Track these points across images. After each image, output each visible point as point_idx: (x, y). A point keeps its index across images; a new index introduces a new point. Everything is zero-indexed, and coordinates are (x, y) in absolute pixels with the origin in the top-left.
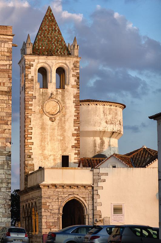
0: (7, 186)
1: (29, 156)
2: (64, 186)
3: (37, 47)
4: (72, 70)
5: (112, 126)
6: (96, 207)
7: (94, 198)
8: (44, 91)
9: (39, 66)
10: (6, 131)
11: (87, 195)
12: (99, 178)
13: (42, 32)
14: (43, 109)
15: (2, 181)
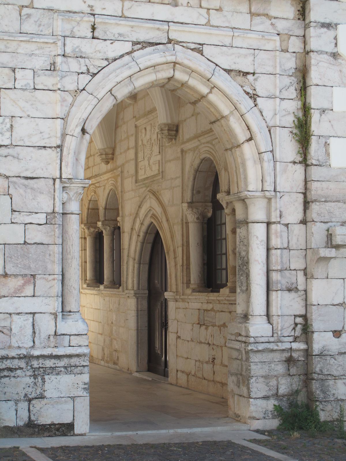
6: (327, 145)
7: (314, 76)
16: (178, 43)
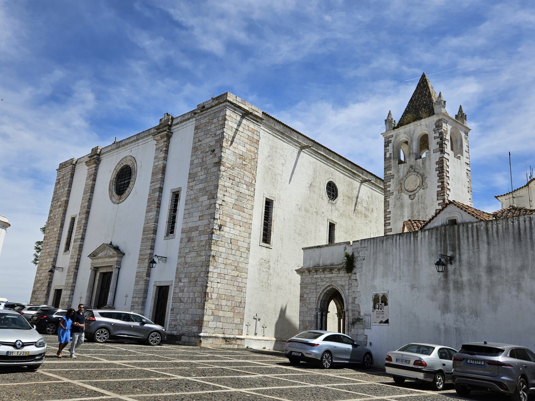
11: (346, 281)
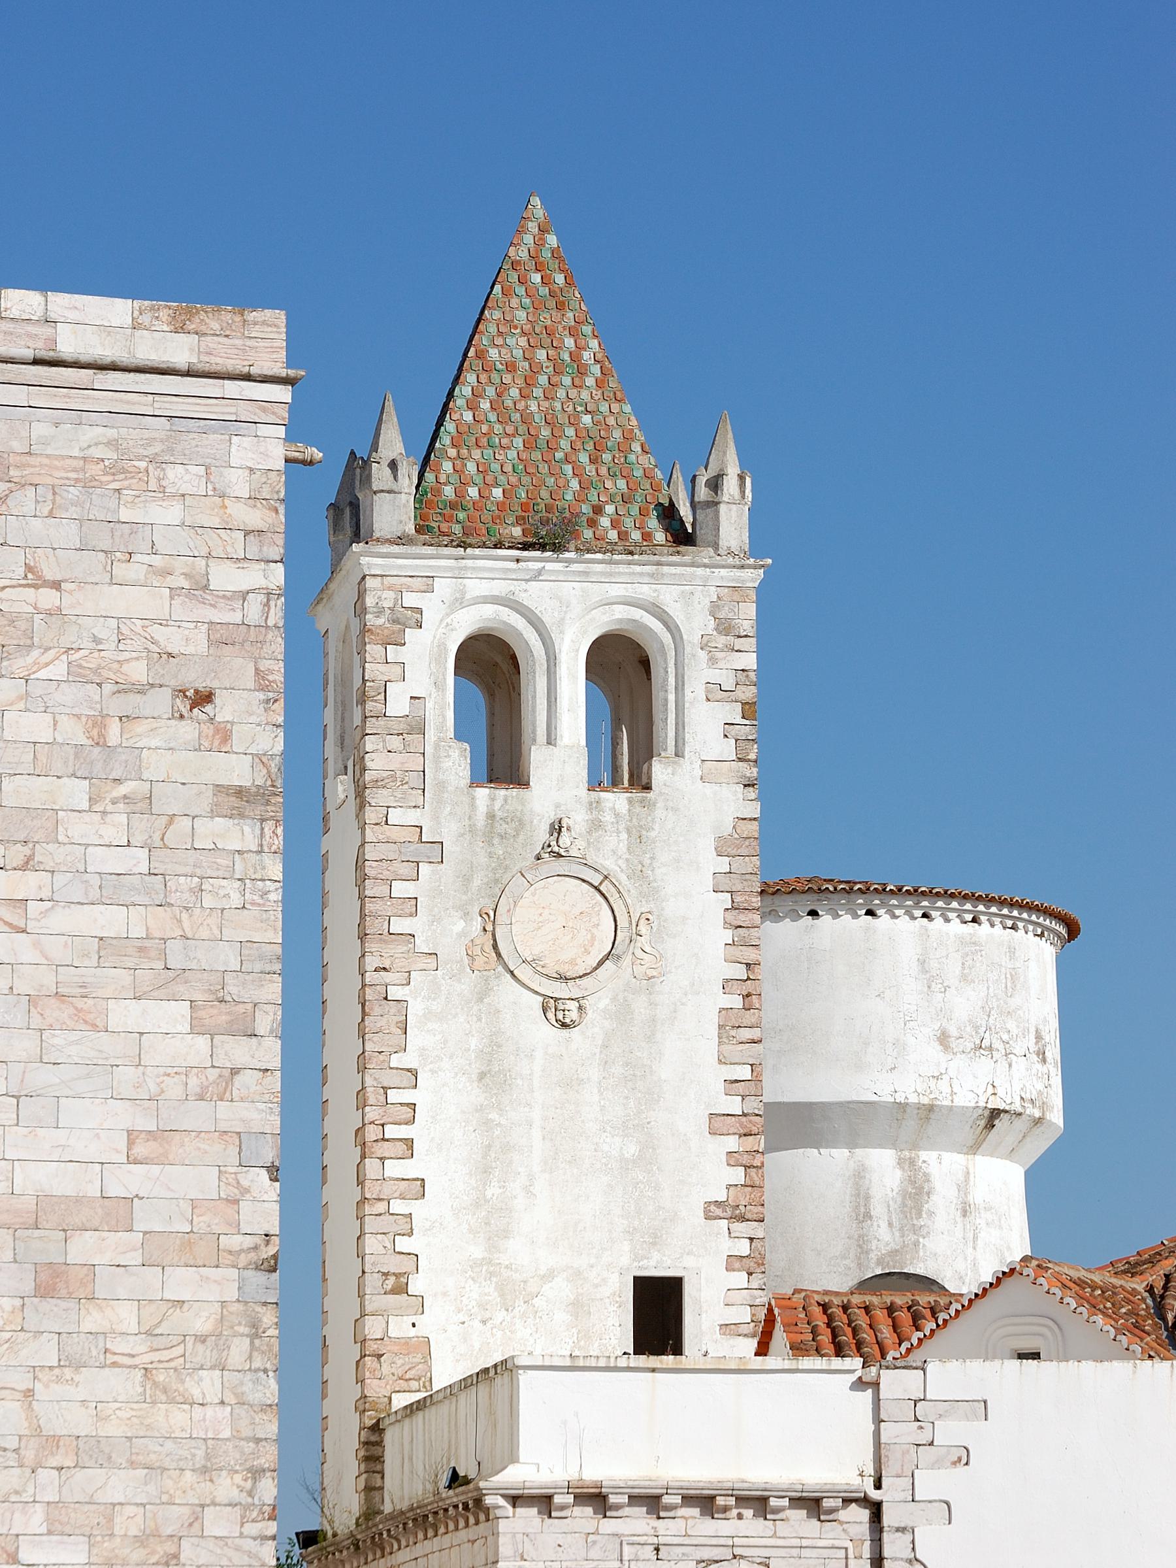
0: (250, 1494)
1: (391, 1281)
2: (666, 1500)
3: (449, 491)
4: (703, 655)
5: (984, 1065)
8: (498, 804)
9: (466, 624)
10: (238, 1079)
12: (924, 1438)
13: (484, 378)
14: (494, 935)
15: (208, 1457)
16: (742, 1557)
